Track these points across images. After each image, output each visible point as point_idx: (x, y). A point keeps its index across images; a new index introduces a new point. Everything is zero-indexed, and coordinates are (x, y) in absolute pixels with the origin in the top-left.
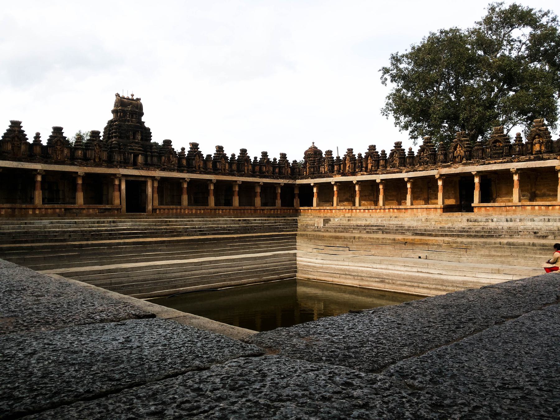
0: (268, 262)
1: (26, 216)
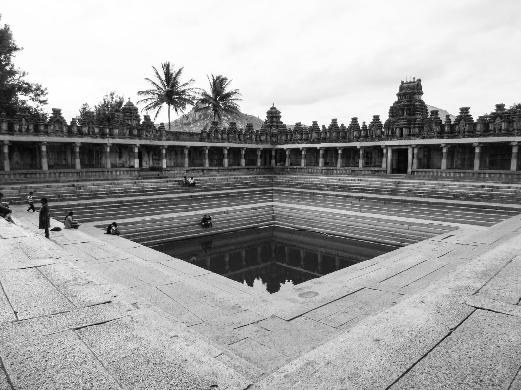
0: (412, 229)
1: (332, 174)
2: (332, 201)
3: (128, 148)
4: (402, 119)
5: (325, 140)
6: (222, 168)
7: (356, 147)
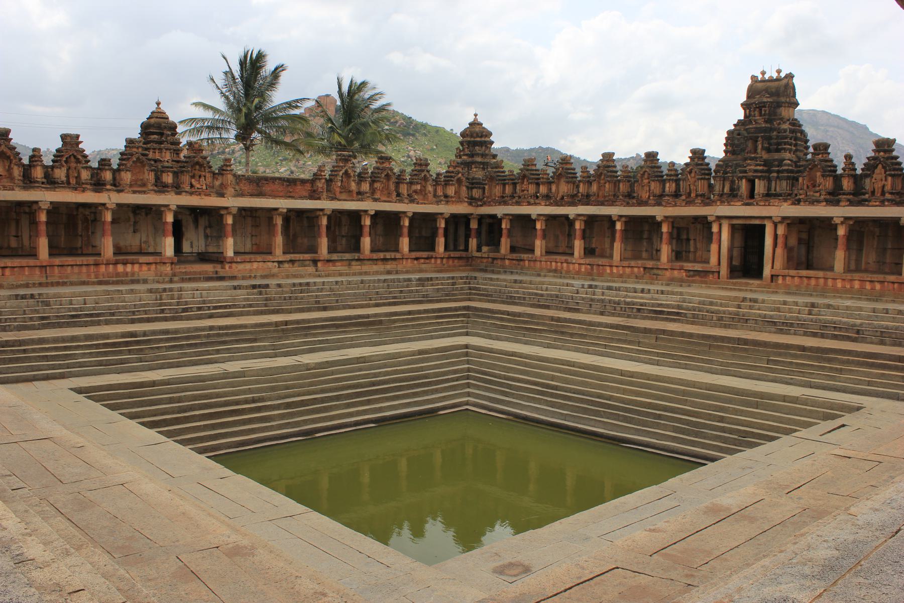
1: (600, 275)
2: (598, 338)
3: (153, 212)
4: (752, 159)
5: (587, 200)
6: (356, 256)
7: (654, 217)
